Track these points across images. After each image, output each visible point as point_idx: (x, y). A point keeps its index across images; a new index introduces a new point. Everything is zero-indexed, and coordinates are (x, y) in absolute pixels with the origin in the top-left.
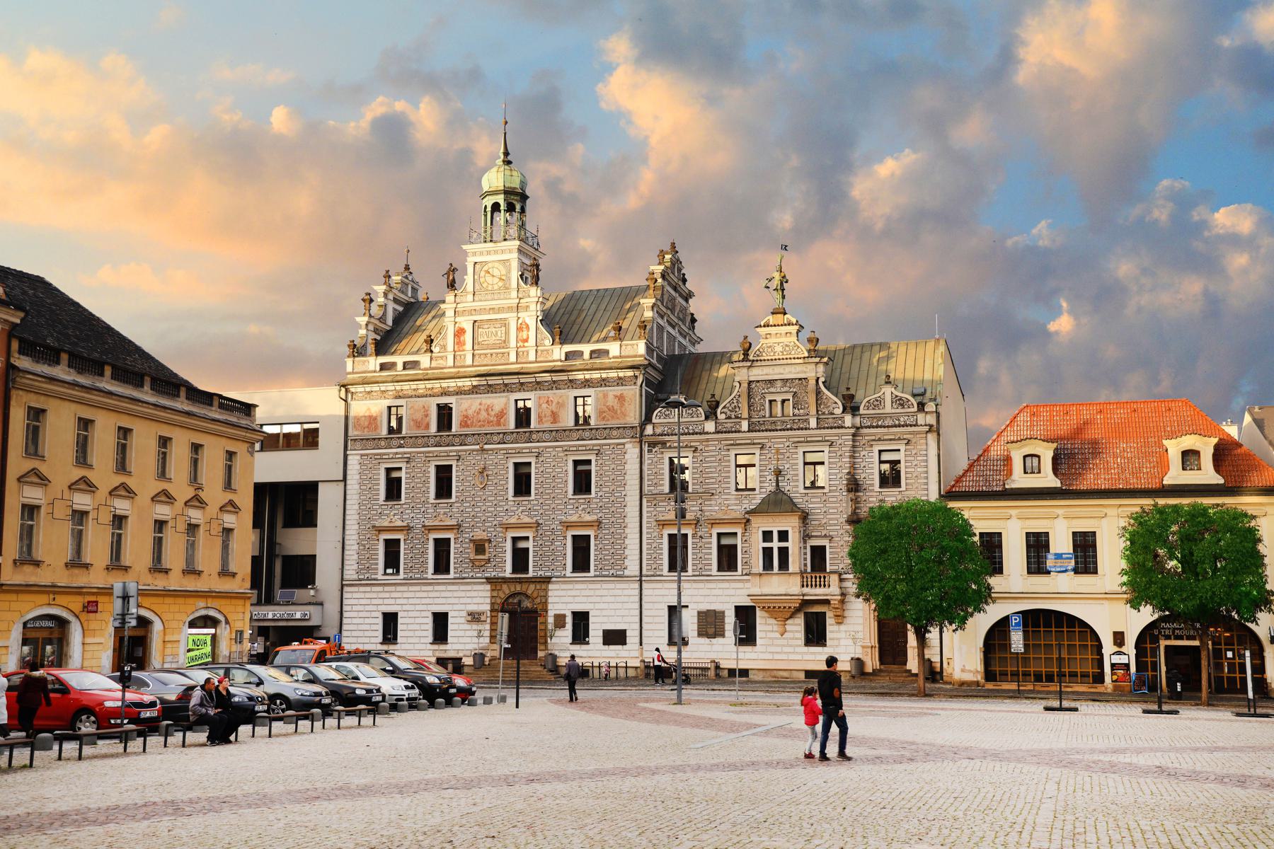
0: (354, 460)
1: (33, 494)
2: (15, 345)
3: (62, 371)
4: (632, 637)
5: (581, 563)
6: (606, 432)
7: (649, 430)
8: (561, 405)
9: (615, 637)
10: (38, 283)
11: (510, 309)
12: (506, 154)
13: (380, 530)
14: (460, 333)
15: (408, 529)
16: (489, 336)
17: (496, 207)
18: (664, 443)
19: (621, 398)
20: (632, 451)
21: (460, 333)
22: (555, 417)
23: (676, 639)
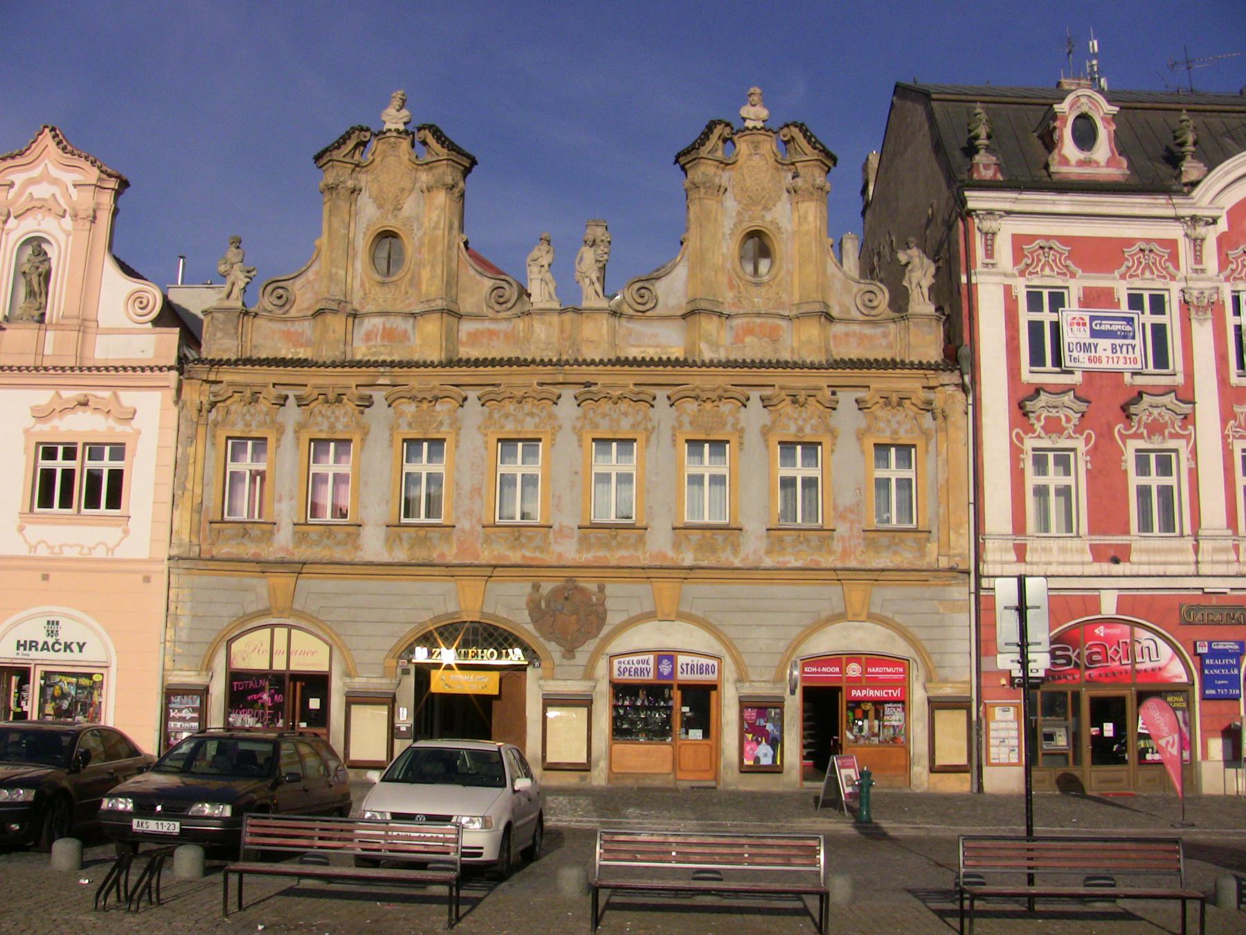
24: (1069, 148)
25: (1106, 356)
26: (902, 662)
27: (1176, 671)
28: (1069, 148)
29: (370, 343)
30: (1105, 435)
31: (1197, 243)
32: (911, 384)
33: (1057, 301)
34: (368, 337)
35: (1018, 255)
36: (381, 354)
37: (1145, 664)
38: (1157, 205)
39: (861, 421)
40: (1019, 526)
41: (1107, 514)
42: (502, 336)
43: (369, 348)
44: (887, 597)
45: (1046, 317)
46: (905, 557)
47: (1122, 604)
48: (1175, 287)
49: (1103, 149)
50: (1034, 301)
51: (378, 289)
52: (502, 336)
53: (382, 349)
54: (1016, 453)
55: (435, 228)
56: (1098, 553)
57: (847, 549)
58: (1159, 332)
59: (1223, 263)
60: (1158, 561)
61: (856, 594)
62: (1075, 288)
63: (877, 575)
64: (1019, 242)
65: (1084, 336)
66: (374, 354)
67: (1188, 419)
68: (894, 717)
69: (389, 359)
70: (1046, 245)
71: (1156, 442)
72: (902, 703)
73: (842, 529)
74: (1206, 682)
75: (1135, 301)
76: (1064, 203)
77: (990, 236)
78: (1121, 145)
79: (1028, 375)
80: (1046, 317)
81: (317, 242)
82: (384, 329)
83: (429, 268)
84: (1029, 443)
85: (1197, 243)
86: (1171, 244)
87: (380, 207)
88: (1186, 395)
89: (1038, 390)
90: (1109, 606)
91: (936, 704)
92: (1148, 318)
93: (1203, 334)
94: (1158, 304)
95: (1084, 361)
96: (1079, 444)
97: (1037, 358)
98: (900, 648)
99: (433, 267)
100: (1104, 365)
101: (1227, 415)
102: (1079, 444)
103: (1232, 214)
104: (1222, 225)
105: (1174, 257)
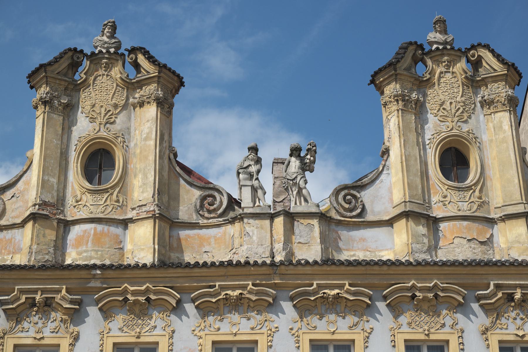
29: (80, 249)
34: (79, 241)
36: (91, 258)
42: (212, 240)
43: (79, 254)
51: (89, 195)
52: (212, 240)
53: (93, 254)
55: (146, 139)
66: (86, 258)
69: (98, 263)
81: (29, 154)
82: (95, 234)
83: (140, 176)
87: (93, 120)
99: (145, 176)
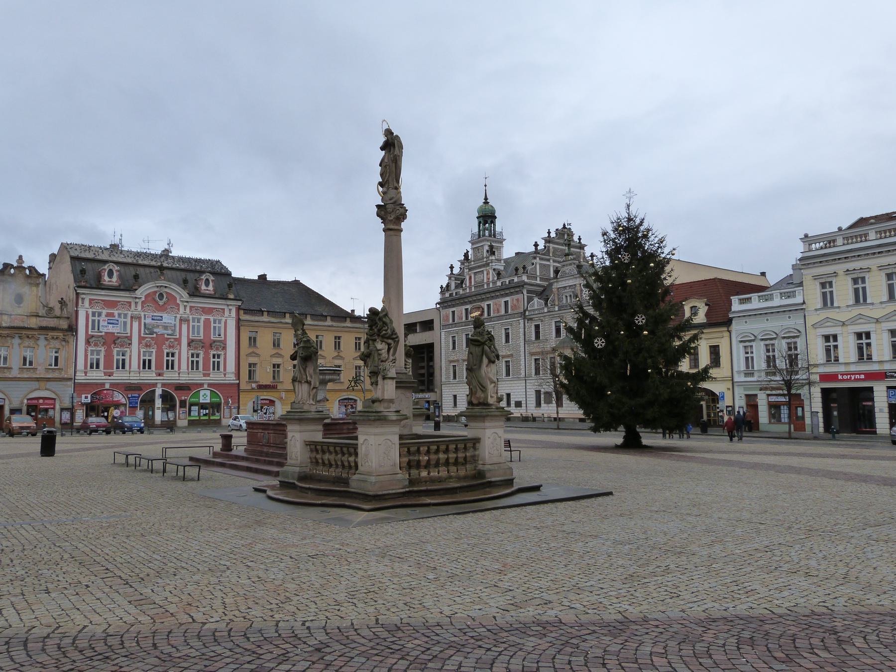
0: (443, 334)
1: (252, 360)
2: (242, 312)
3: (265, 318)
4: (524, 405)
5: (508, 374)
6: (513, 316)
7: (527, 313)
8: (500, 305)
9: (518, 404)
10: (296, 283)
11: (484, 266)
12: (486, 199)
13: (451, 362)
14: (470, 278)
15: (458, 361)
16: (479, 278)
17: (480, 223)
18: (531, 319)
19: (518, 300)
20: (522, 322)
21: (470, 278)
22: (498, 311)
23: (538, 404)
24: (106, 278)
25: (111, 329)
26: (54, 399)
27: (123, 401)
28: (106, 278)
30: (109, 347)
31: (136, 303)
32: (61, 335)
33: (100, 314)
35: (90, 303)
37: (116, 399)
38: (127, 294)
39: (46, 343)
40: (86, 367)
41: (109, 365)
44: (50, 385)
45: (96, 318)
46: (56, 375)
47: (112, 385)
48: (130, 313)
49: (115, 279)
50: (94, 314)
54: (86, 351)
56: (105, 374)
57: (41, 373)
58: (125, 323)
59: (143, 307)
60: (119, 376)
61: (43, 384)
62: (104, 312)
63: (49, 380)
64: (91, 300)
65: (106, 324)
67: (130, 344)
68: (51, 413)
70: (97, 302)
71: (122, 349)
72: (54, 408)
73: (39, 368)
74: (130, 403)
75: (119, 315)
76: (103, 292)
77: (83, 299)
78: (120, 277)
79: (90, 333)
80: (96, 318)
84: (90, 348)
85: (136, 303)
86: (130, 303)
88: (130, 338)
89: (93, 336)
90: (107, 386)
91: (62, 410)
92: (123, 320)
93: (136, 325)
94: (125, 316)
95: (105, 330)
96: (103, 349)
97: (93, 328)
98: (53, 396)
100: (110, 331)
101: (140, 343)
102: (103, 349)
103: (146, 296)
104: (143, 299)
105: (130, 306)
